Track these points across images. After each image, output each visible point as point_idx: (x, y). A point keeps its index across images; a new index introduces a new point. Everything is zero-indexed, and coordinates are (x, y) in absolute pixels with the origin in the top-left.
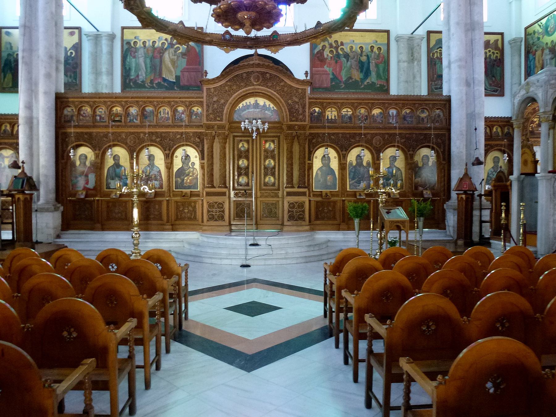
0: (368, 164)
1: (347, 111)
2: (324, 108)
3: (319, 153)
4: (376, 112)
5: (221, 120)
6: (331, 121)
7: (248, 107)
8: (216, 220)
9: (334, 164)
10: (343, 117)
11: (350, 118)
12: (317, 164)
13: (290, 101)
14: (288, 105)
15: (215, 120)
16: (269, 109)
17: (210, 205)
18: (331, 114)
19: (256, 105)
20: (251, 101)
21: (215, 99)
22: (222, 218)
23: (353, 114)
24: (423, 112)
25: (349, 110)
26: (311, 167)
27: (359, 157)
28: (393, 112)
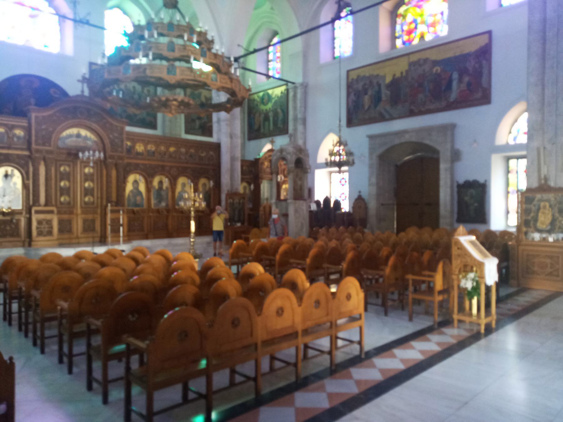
0: (167, 188)
1: (151, 147)
2: (134, 142)
3: (131, 178)
4: (172, 149)
5: (50, 146)
6: (138, 154)
7: (70, 136)
8: (45, 236)
9: (142, 188)
10: (148, 152)
11: (154, 153)
12: (129, 187)
13: (111, 136)
14: (109, 138)
15: (44, 144)
16: (89, 139)
17: (40, 222)
18: (140, 148)
19: (78, 135)
20: (74, 131)
21: (43, 127)
22: (50, 233)
23: (156, 150)
24: (202, 152)
25: (153, 146)
26: (124, 190)
27: (161, 183)
28: (183, 150)
